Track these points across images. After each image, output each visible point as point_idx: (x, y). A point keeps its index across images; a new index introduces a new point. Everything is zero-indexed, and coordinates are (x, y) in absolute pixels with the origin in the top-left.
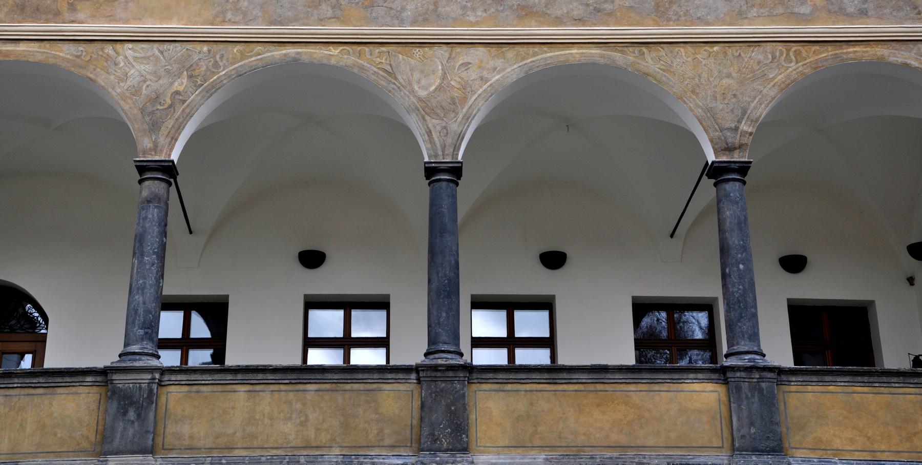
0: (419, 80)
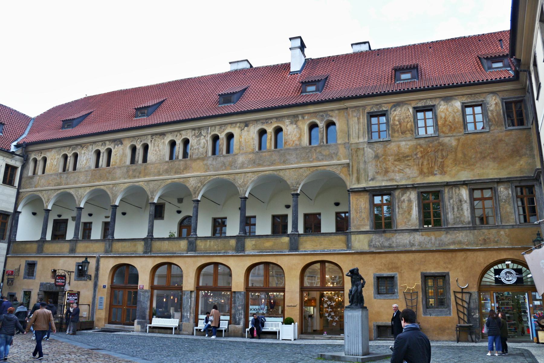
0: (239, 181)
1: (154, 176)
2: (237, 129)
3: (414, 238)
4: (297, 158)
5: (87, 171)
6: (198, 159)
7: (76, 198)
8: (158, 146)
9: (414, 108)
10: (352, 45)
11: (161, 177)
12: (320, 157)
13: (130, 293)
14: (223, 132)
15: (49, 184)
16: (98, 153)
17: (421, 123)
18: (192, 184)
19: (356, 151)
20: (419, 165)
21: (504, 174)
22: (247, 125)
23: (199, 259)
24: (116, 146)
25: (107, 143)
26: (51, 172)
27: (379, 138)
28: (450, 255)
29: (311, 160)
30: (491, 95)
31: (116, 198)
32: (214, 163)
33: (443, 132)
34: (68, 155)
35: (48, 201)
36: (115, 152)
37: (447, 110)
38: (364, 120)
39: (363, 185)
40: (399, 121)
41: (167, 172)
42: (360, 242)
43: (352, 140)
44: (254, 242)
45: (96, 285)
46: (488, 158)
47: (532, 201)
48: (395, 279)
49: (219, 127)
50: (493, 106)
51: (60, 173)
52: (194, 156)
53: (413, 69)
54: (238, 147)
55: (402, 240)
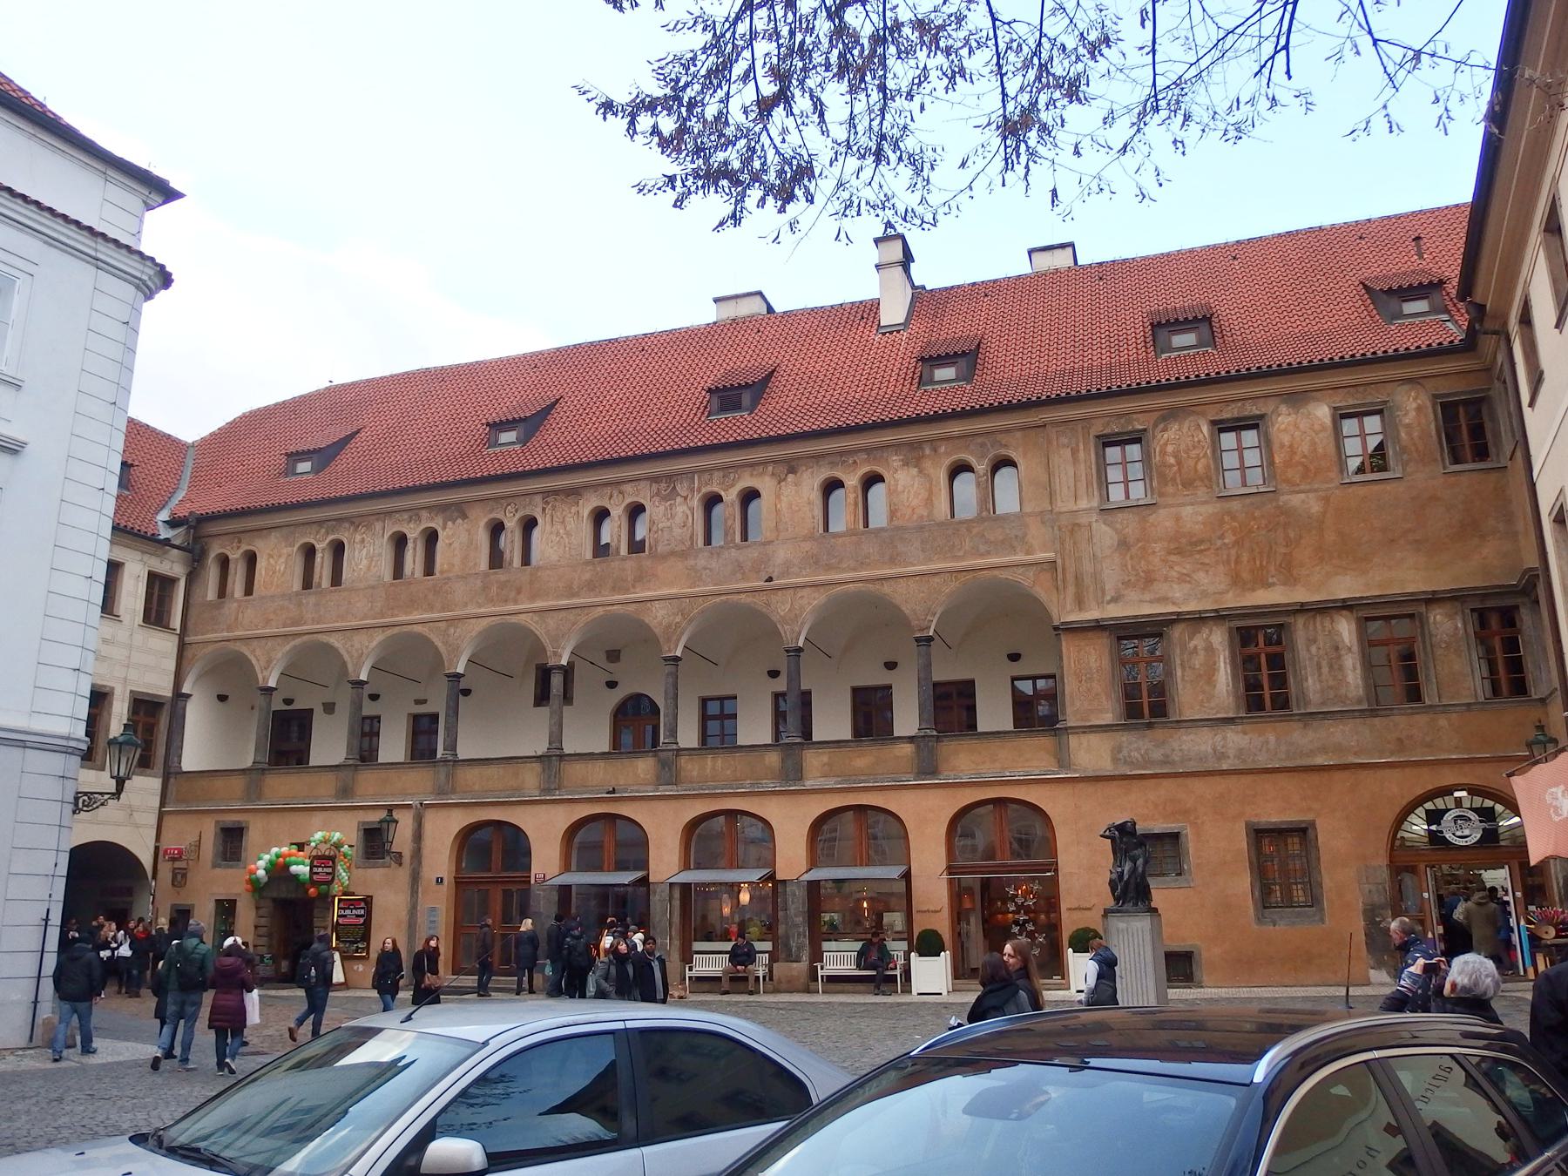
0: (781, 607)
1: (558, 598)
2: (767, 479)
3: (1224, 738)
5: (373, 587)
6: (672, 553)
7: (346, 657)
9: (1213, 423)
10: (1030, 252)
12: (982, 548)
13: (507, 895)
14: (732, 486)
16: (400, 541)
17: (1230, 460)
18: (658, 617)
19: (1072, 532)
20: (1228, 562)
21: (1442, 582)
22: (792, 470)
23: (687, 802)
25: (424, 514)
28: (1315, 778)
30: (1406, 387)
31: (458, 658)
32: (714, 564)
33: (1288, 481)
36: (448, 537)
37: (1296, 426)
38: (1088, 455)
40: (1176, 455)
41: (591, 587)
42: (1091, 754)
43: (1059, 504)
44: (825, 759)
45: (415, 878)
46: (1402, 542)
47: (1512, 645)
48: (1182, 839)
49: (721, 474)
50: (1413, 414)
51: (297, 594)
53: (1202, 321)
55: (1195, 745)
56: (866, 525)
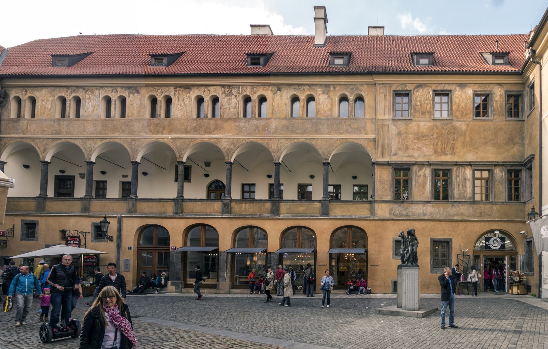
1: (181, 133)
4: (328, 129)
5: (95, 120)
6: (230, 119)
8: (183, 100)
11: (189, 135)
12: (350, 130)
15: (43, 131)
16: (108, 101)
17: (438, 107)
21: (500, 159)
24: (131, 95)
25: (119, 89)
26: (45, 117)
27: (402, 116)
29: (342, 131)
32: (247, 125)
33: (456, 117)
34: (67, 98)
35: (45, 151)
39: (386, 159)
51: (58, 120)
52: (225, 116)
54: (271, 112)
56: (307, 116)
